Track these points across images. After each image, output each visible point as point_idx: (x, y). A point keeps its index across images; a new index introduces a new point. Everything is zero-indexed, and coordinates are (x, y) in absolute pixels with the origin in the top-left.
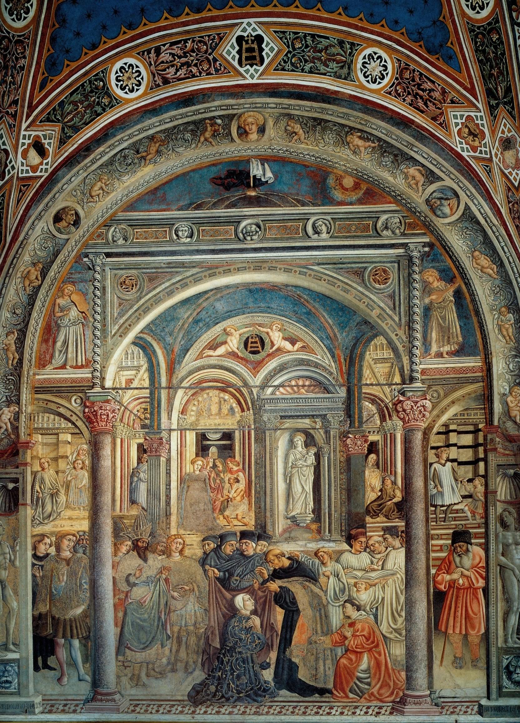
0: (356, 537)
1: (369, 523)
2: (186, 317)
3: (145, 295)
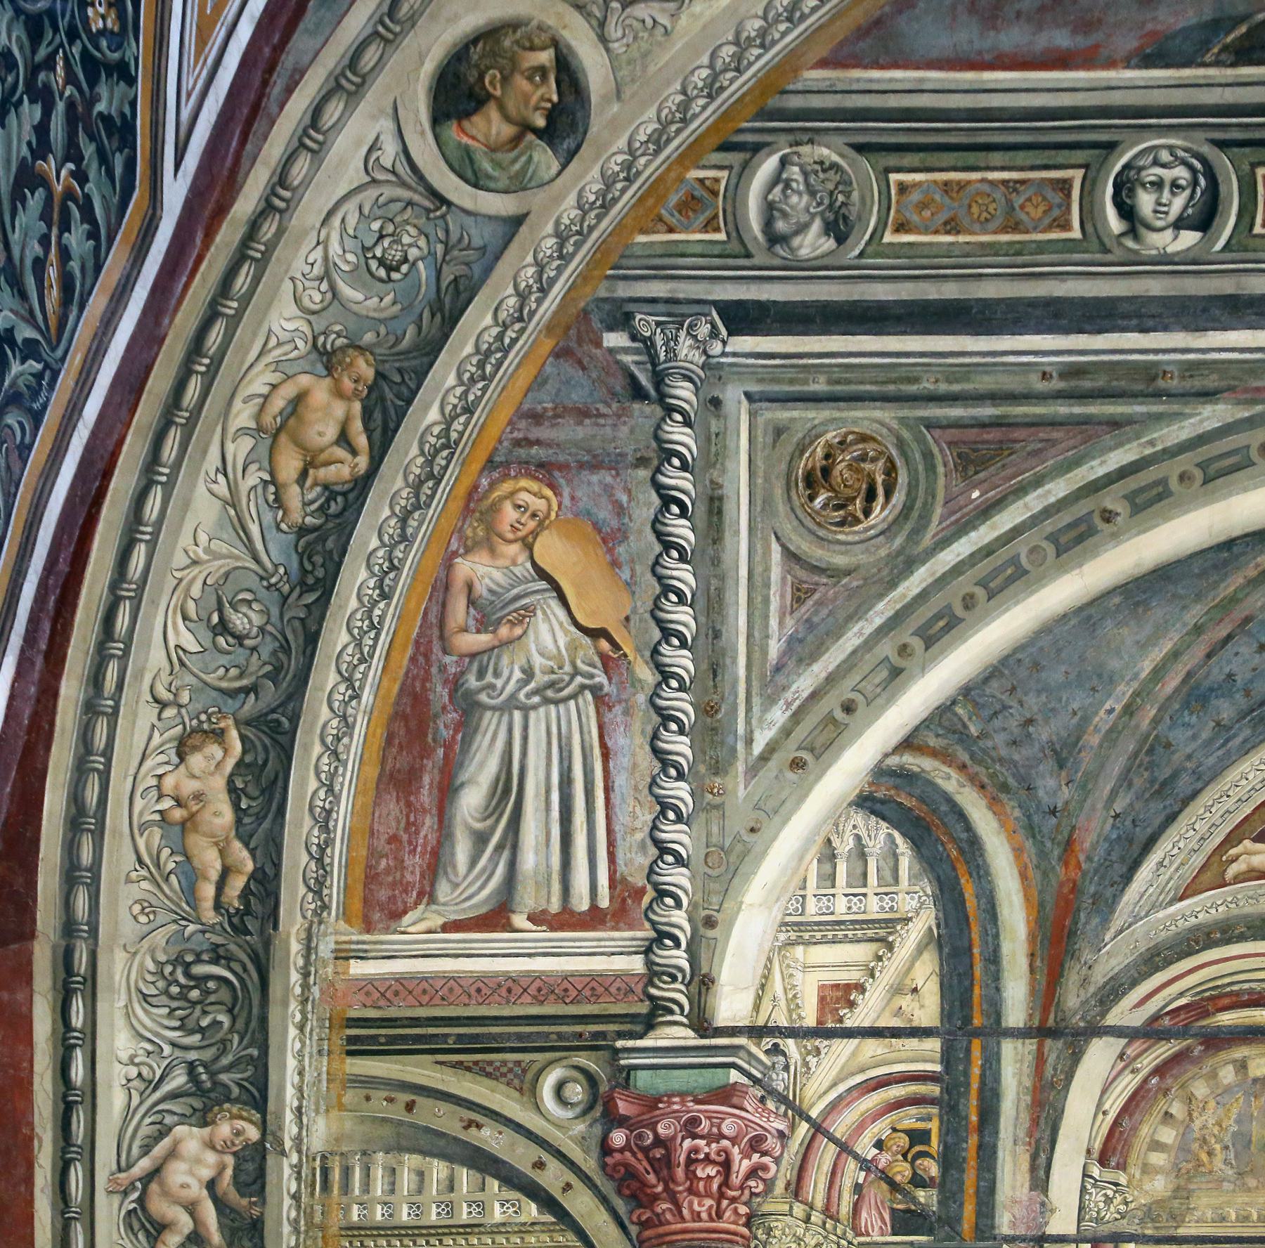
2: (1147, 666)
3: (943, 543)
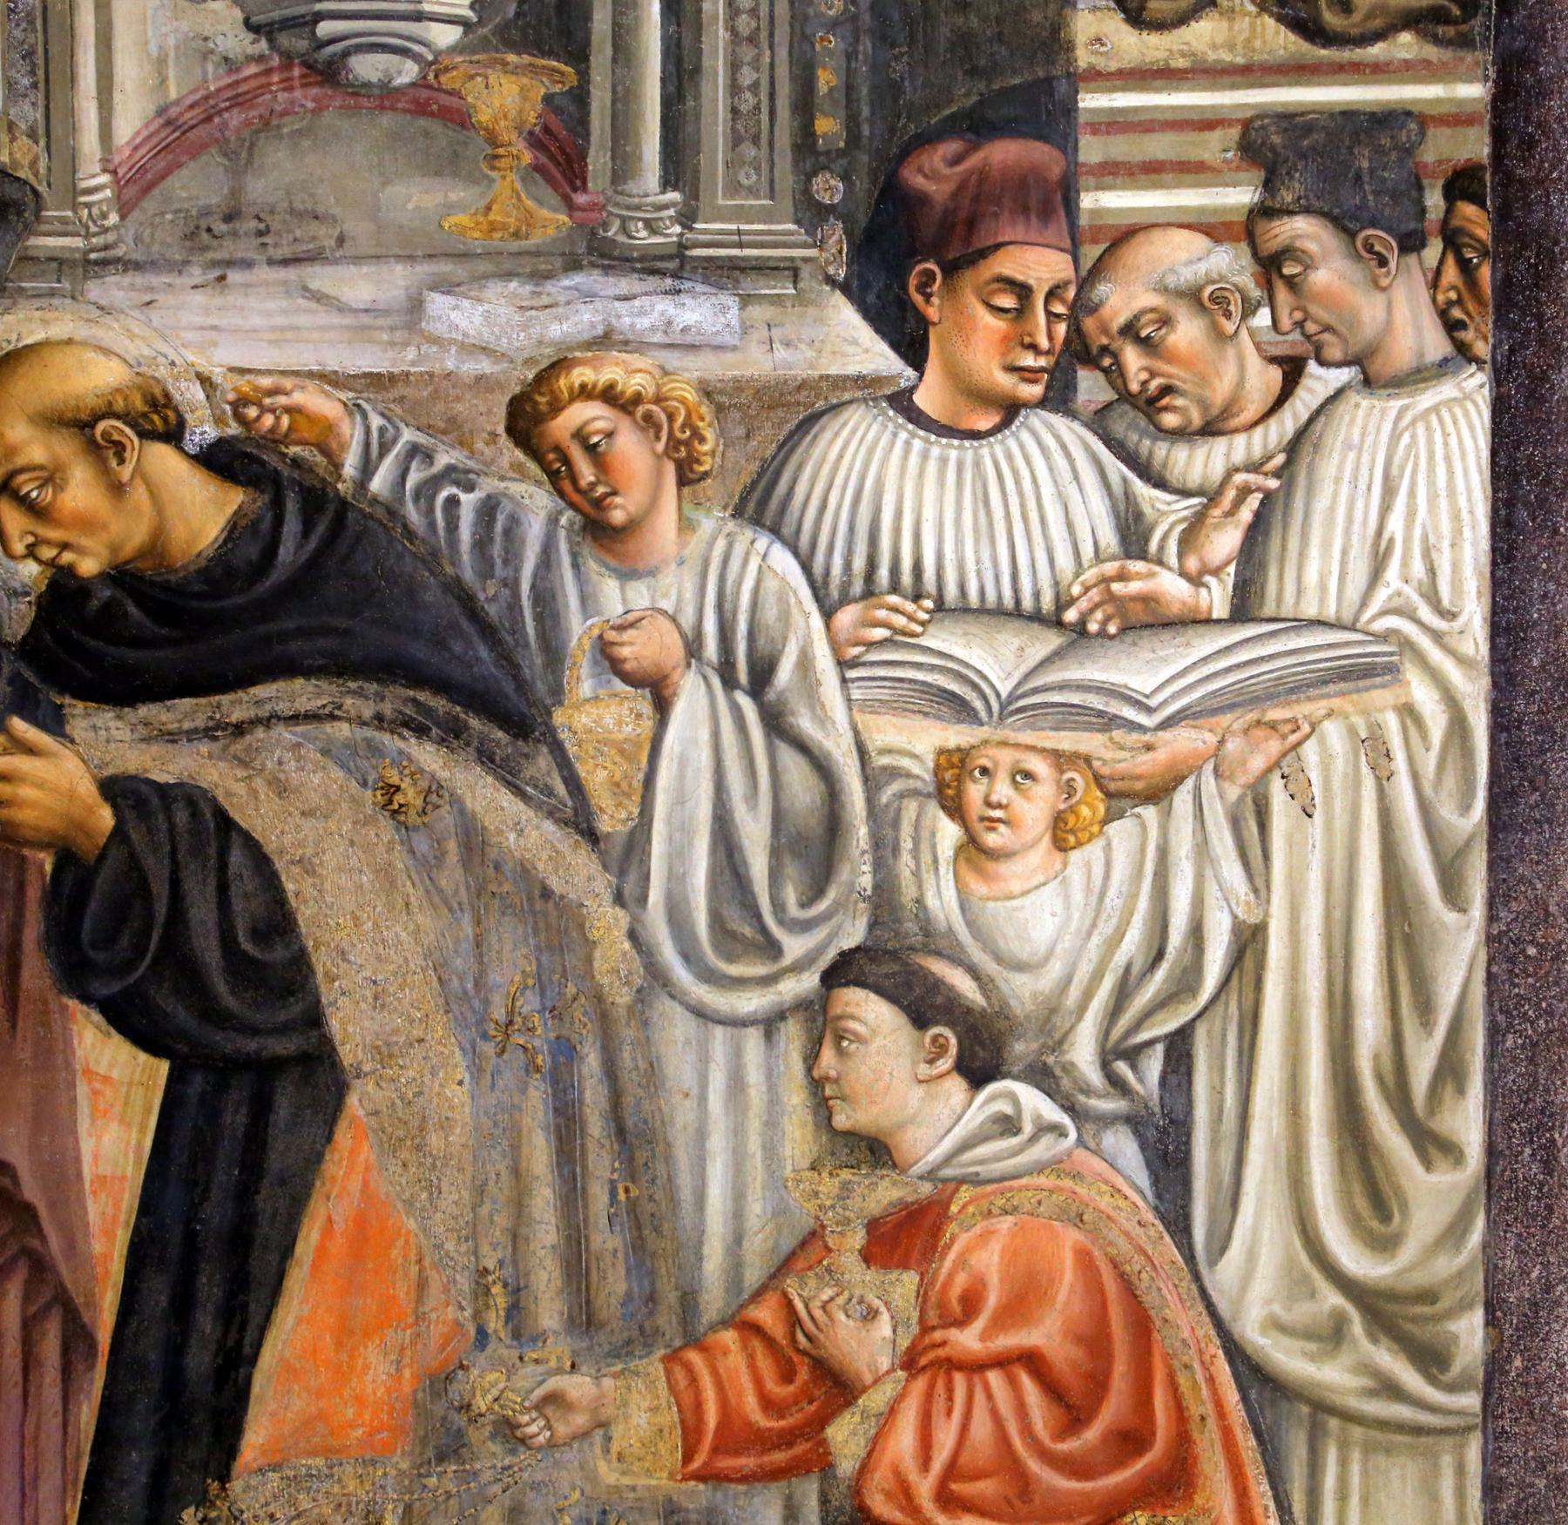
0: (958, 241)
1: (1098, 78)
